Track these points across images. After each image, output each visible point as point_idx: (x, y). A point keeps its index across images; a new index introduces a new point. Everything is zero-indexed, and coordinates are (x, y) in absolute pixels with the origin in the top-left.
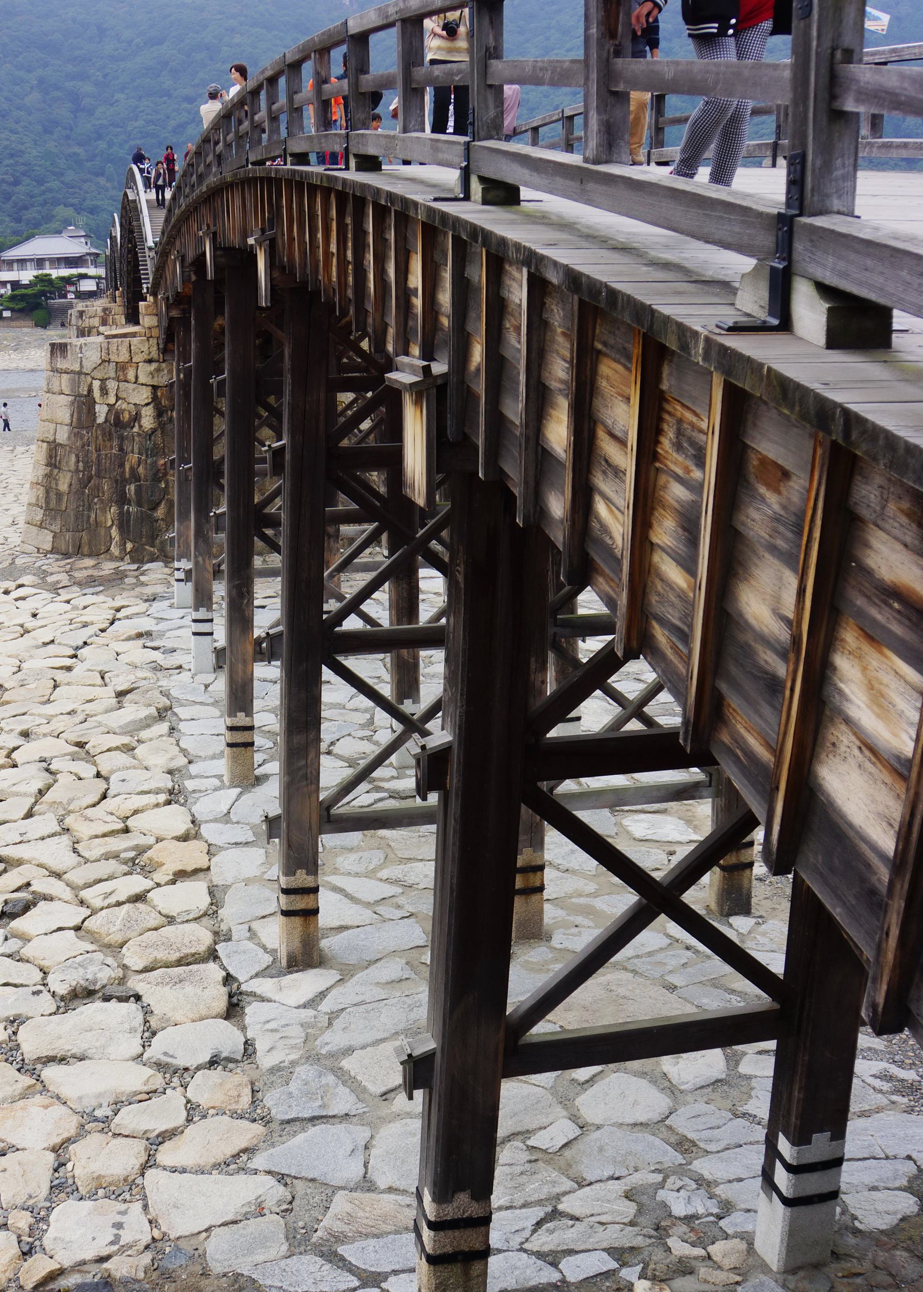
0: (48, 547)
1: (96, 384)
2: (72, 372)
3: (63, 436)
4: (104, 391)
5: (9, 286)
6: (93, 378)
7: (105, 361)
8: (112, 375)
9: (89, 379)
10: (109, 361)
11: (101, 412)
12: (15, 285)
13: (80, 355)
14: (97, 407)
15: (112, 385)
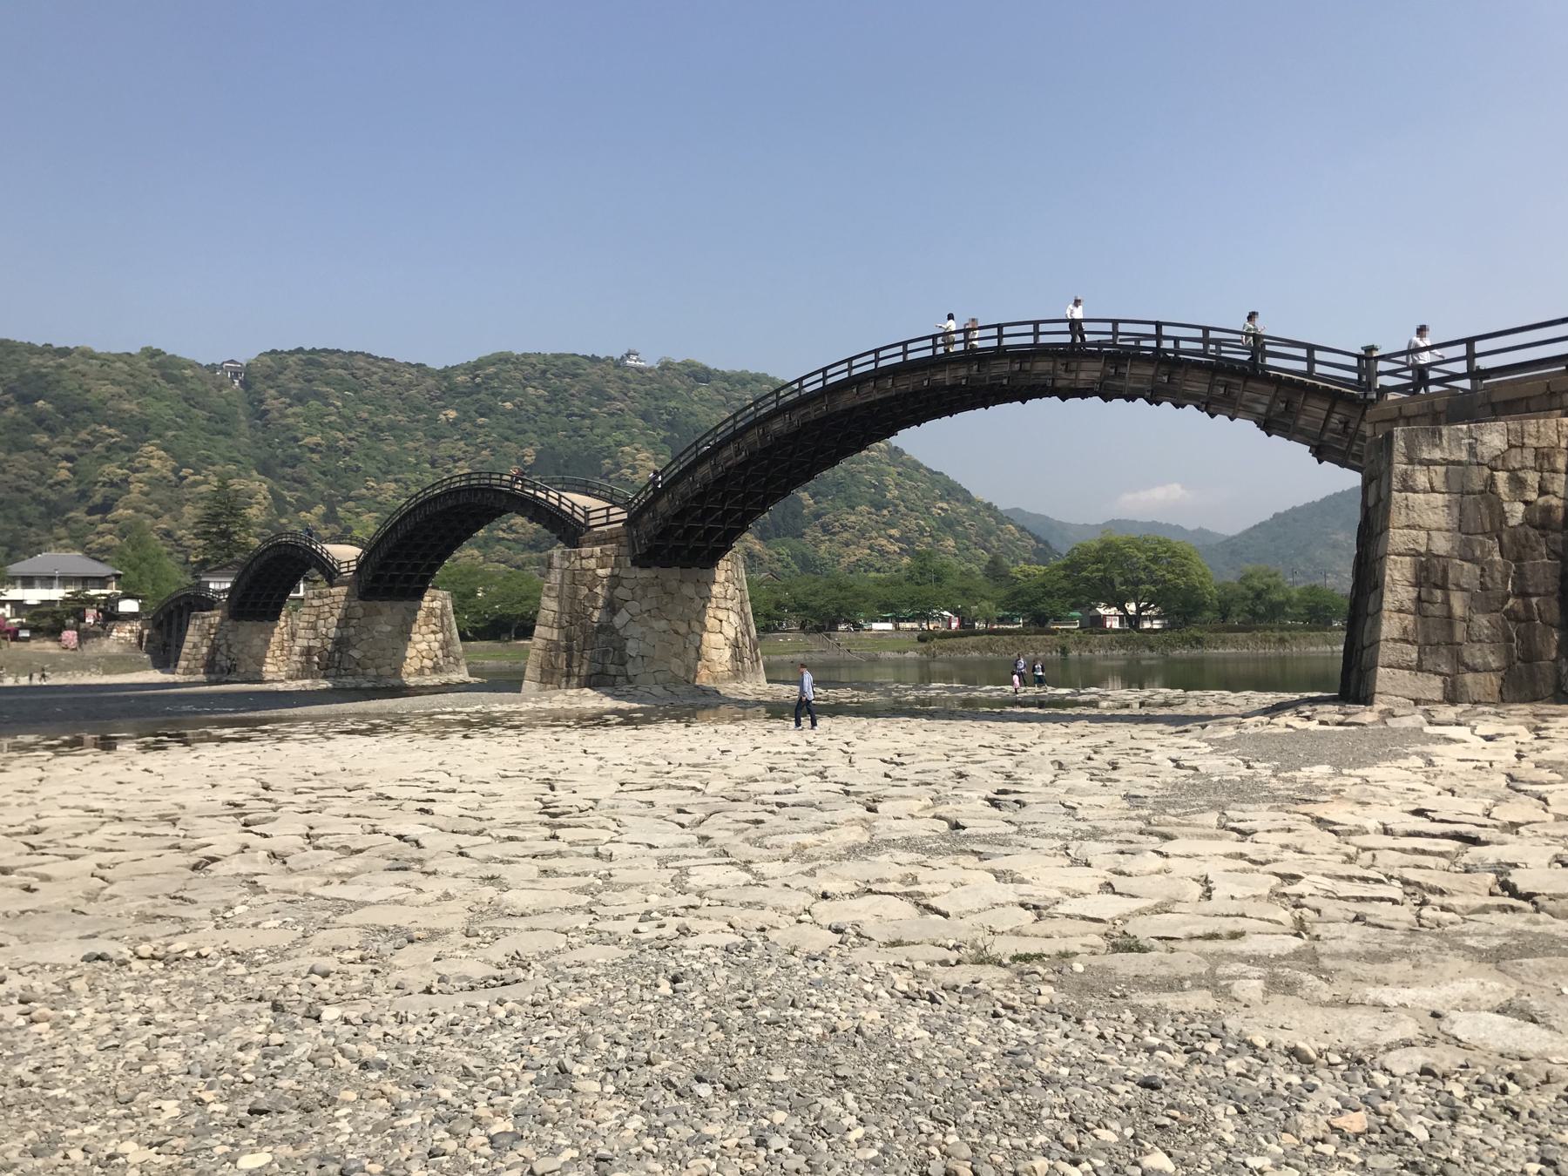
0: (1438, 695)
1: (1501, 477)
2: (1453, 463)
3: (1441, 545)
4: (1517, 483)
5: (8, 606)
6: (1494, 469)
7: (1515, 447)
8: (1530, 462)
9: (1487, 471)
10: (1523, 446)
11: (1516, 512)
12: (18, 605)
13: (1466, 441)
14: (1506, 507)
15: (1532, 478)
